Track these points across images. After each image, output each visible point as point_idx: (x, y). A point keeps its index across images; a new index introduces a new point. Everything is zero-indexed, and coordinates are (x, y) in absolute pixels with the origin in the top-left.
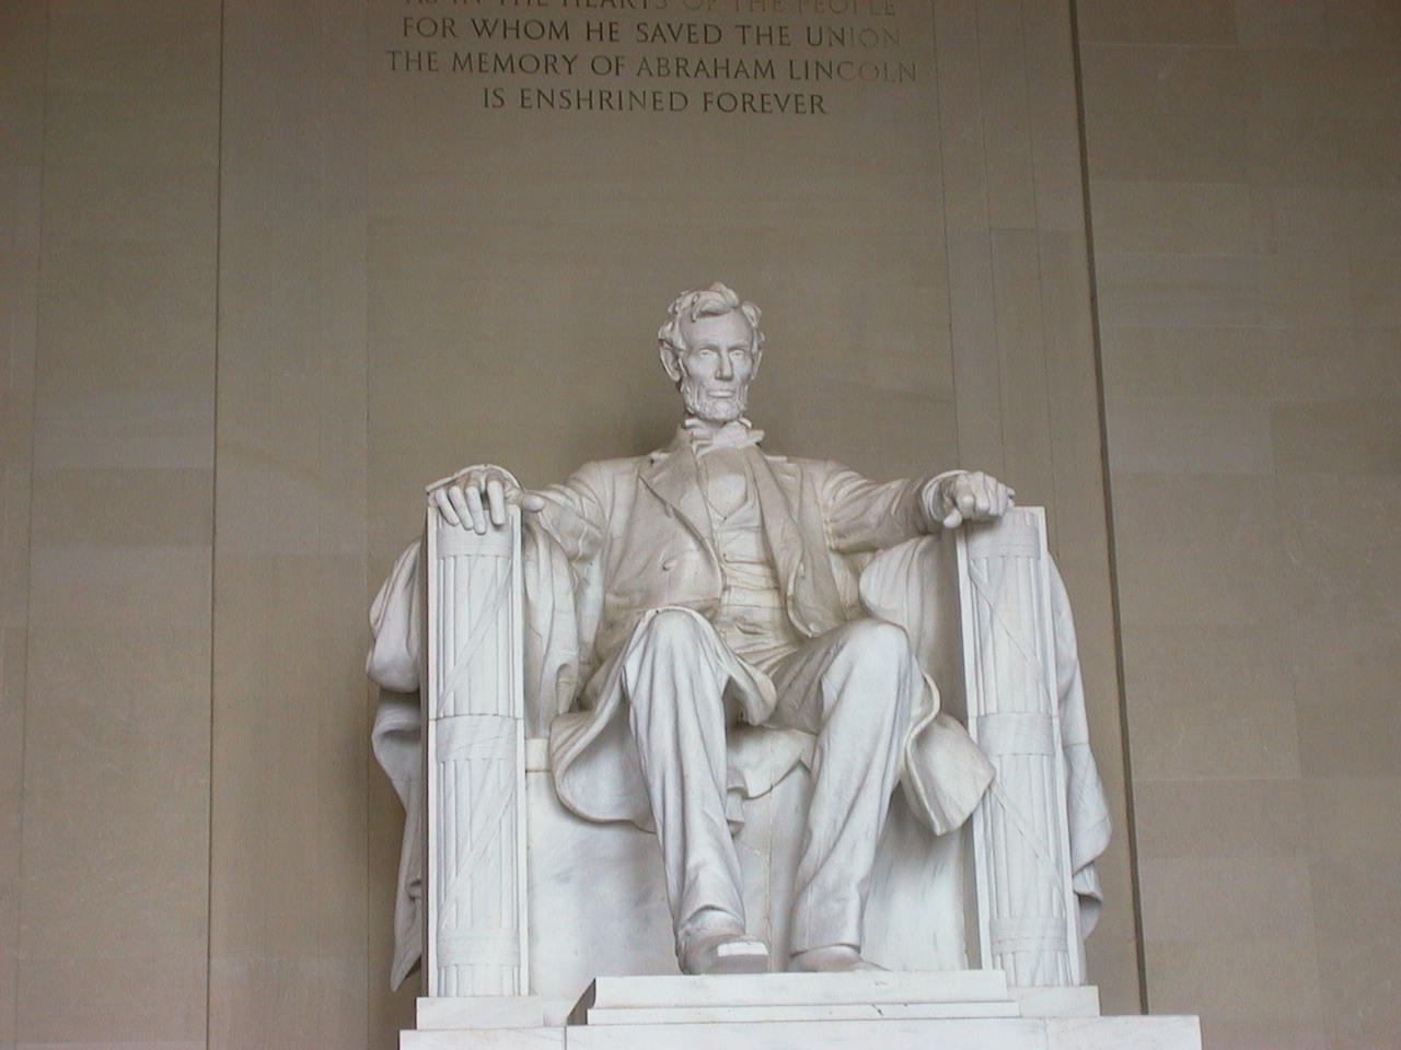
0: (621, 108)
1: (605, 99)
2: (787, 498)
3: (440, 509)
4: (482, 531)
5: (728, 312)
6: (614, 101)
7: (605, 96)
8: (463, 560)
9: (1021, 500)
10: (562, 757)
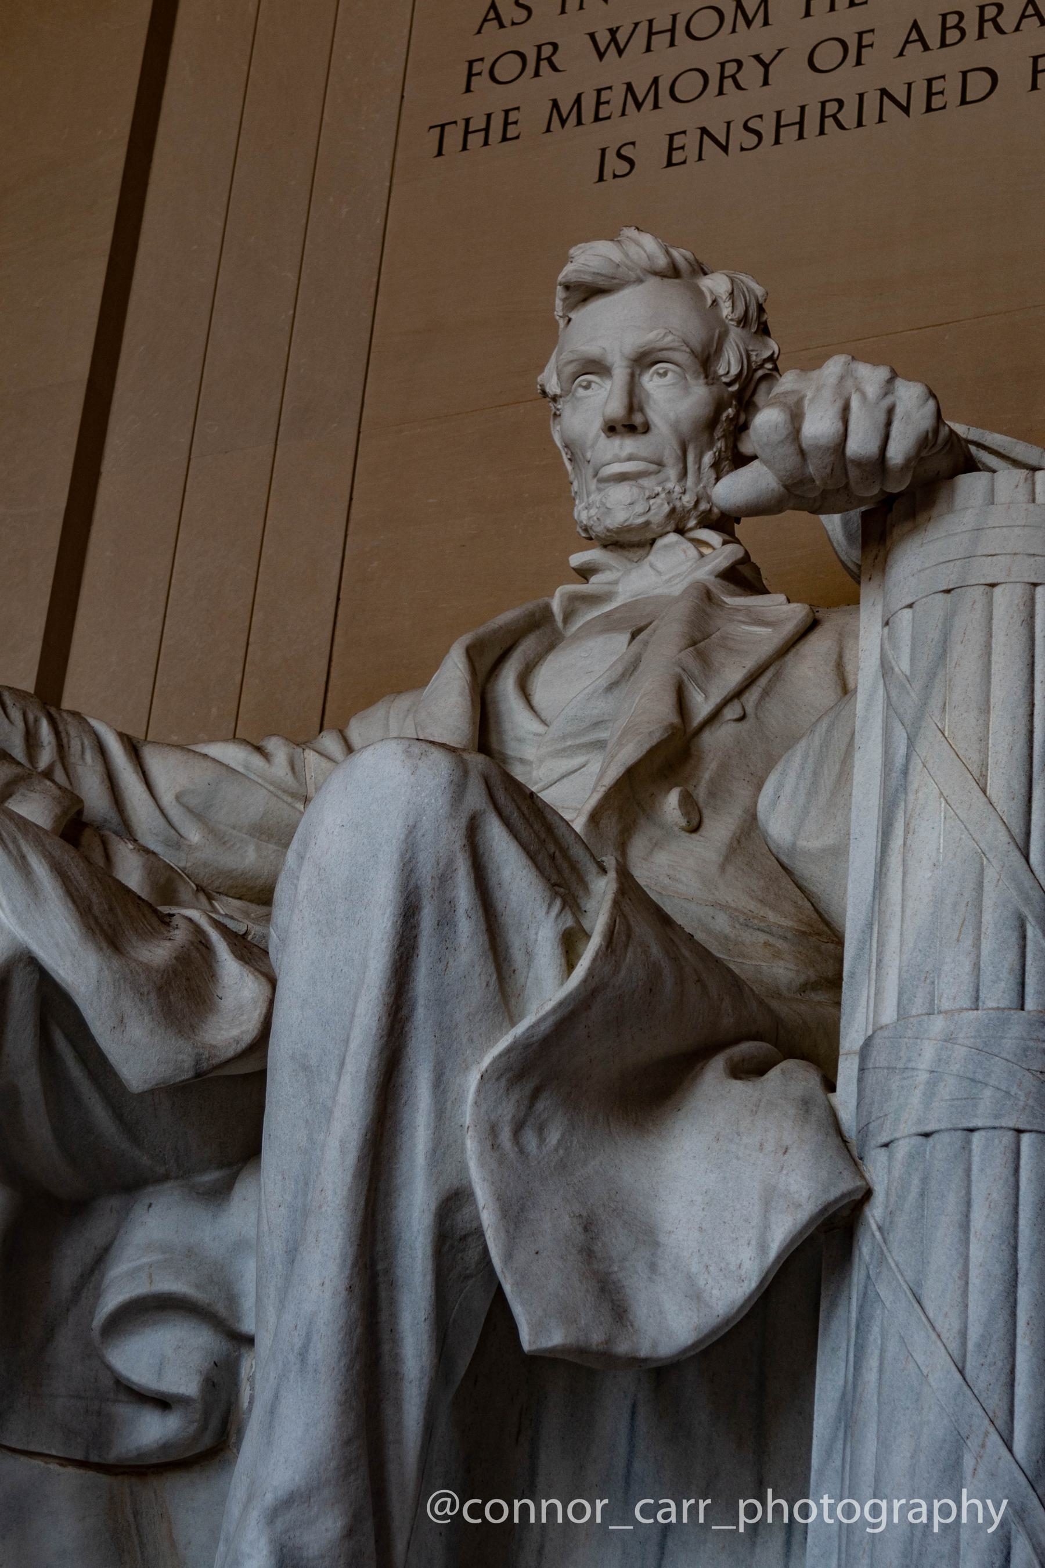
0: (860, 124)
1: (830, 115)
2: (704, 658)
5: (640, 281)
6: (848, 116)
7: (831, 108)
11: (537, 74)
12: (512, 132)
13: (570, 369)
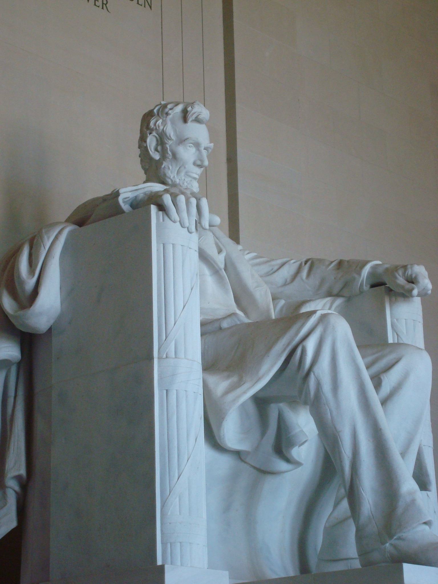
3: (161, 208)
8: (179, 249)
10: (234, 401)
13: (192, 142)
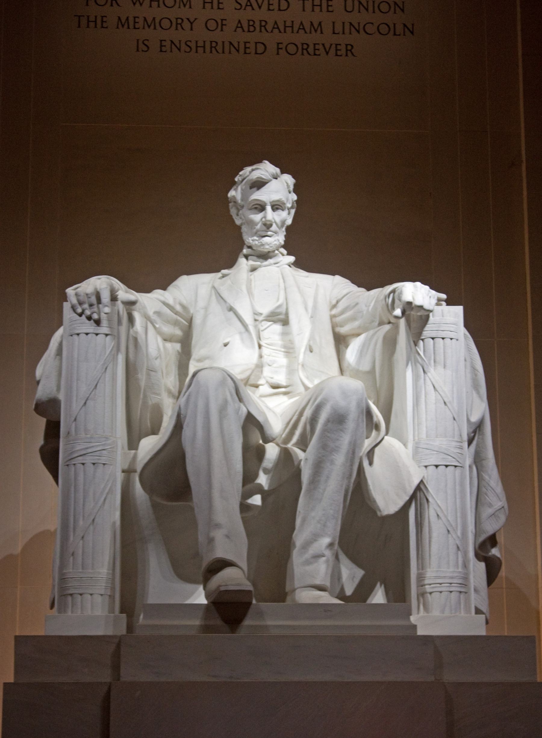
0: (223, 52)
4: (95, 316)
5: (271, 180)
7: (214, 44)
9: (450, 302)
11: (112, 5)
12: (105, 25)
